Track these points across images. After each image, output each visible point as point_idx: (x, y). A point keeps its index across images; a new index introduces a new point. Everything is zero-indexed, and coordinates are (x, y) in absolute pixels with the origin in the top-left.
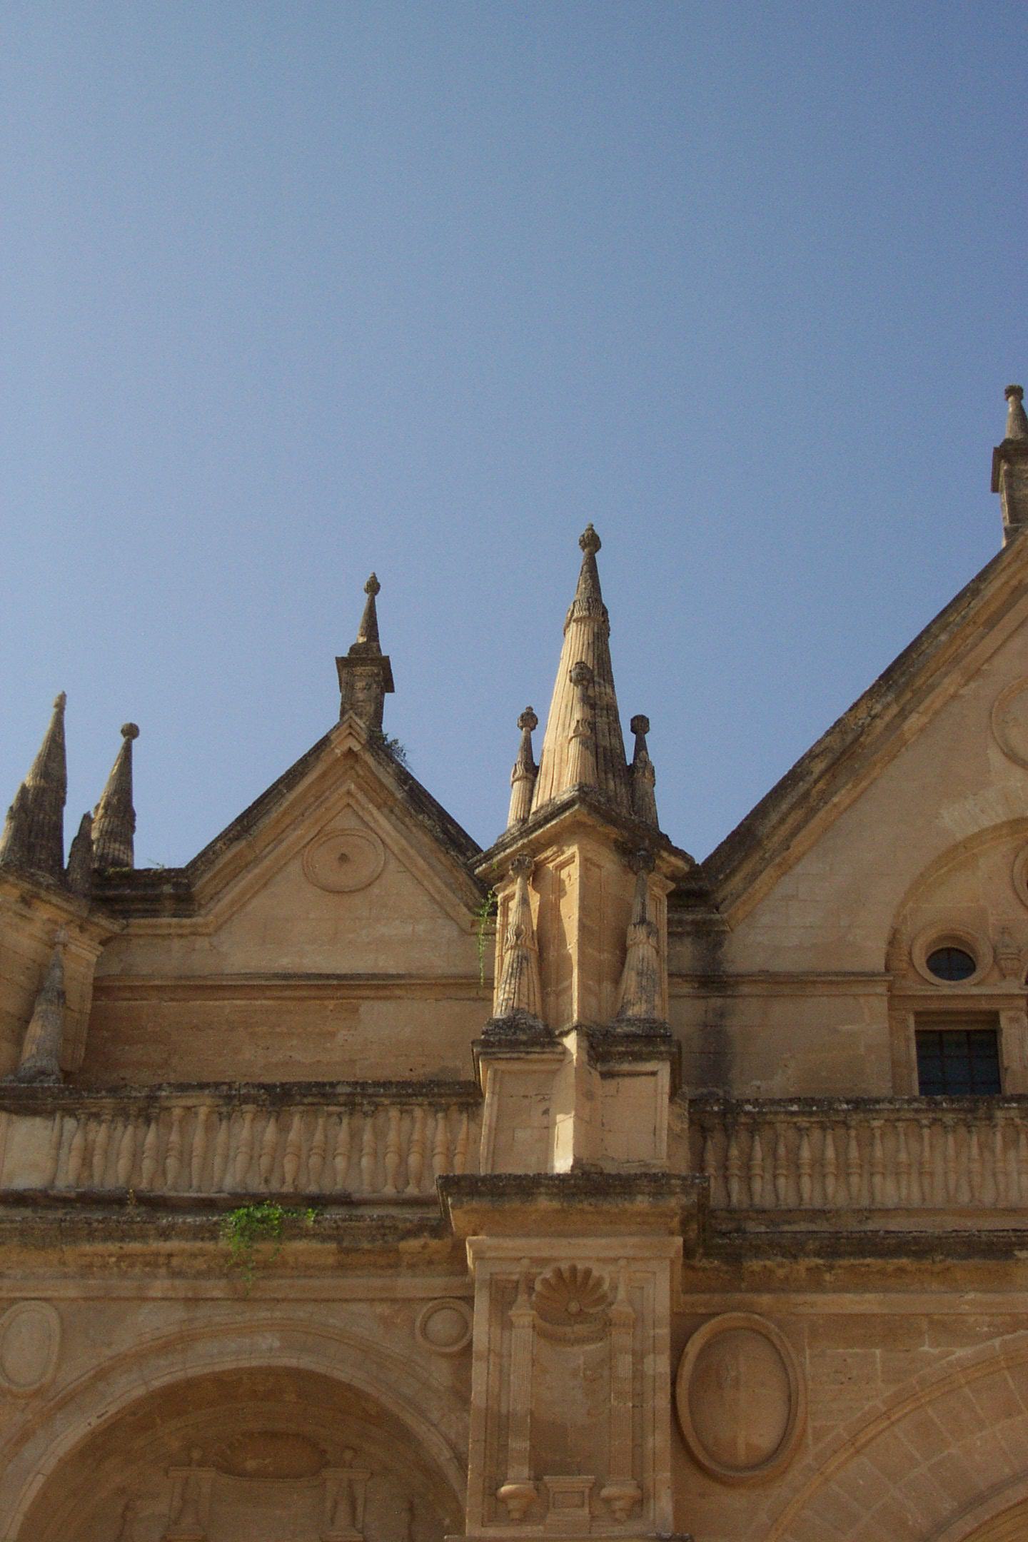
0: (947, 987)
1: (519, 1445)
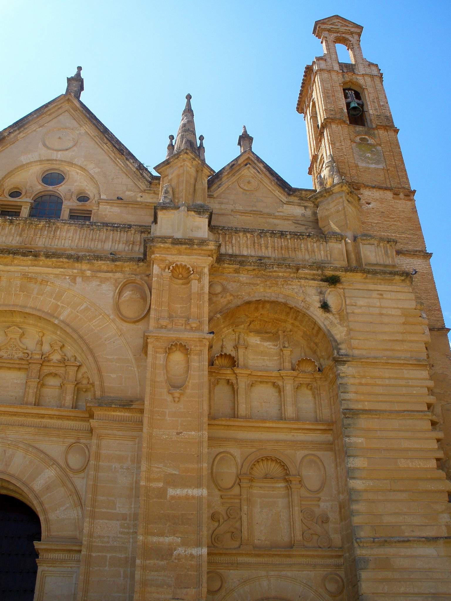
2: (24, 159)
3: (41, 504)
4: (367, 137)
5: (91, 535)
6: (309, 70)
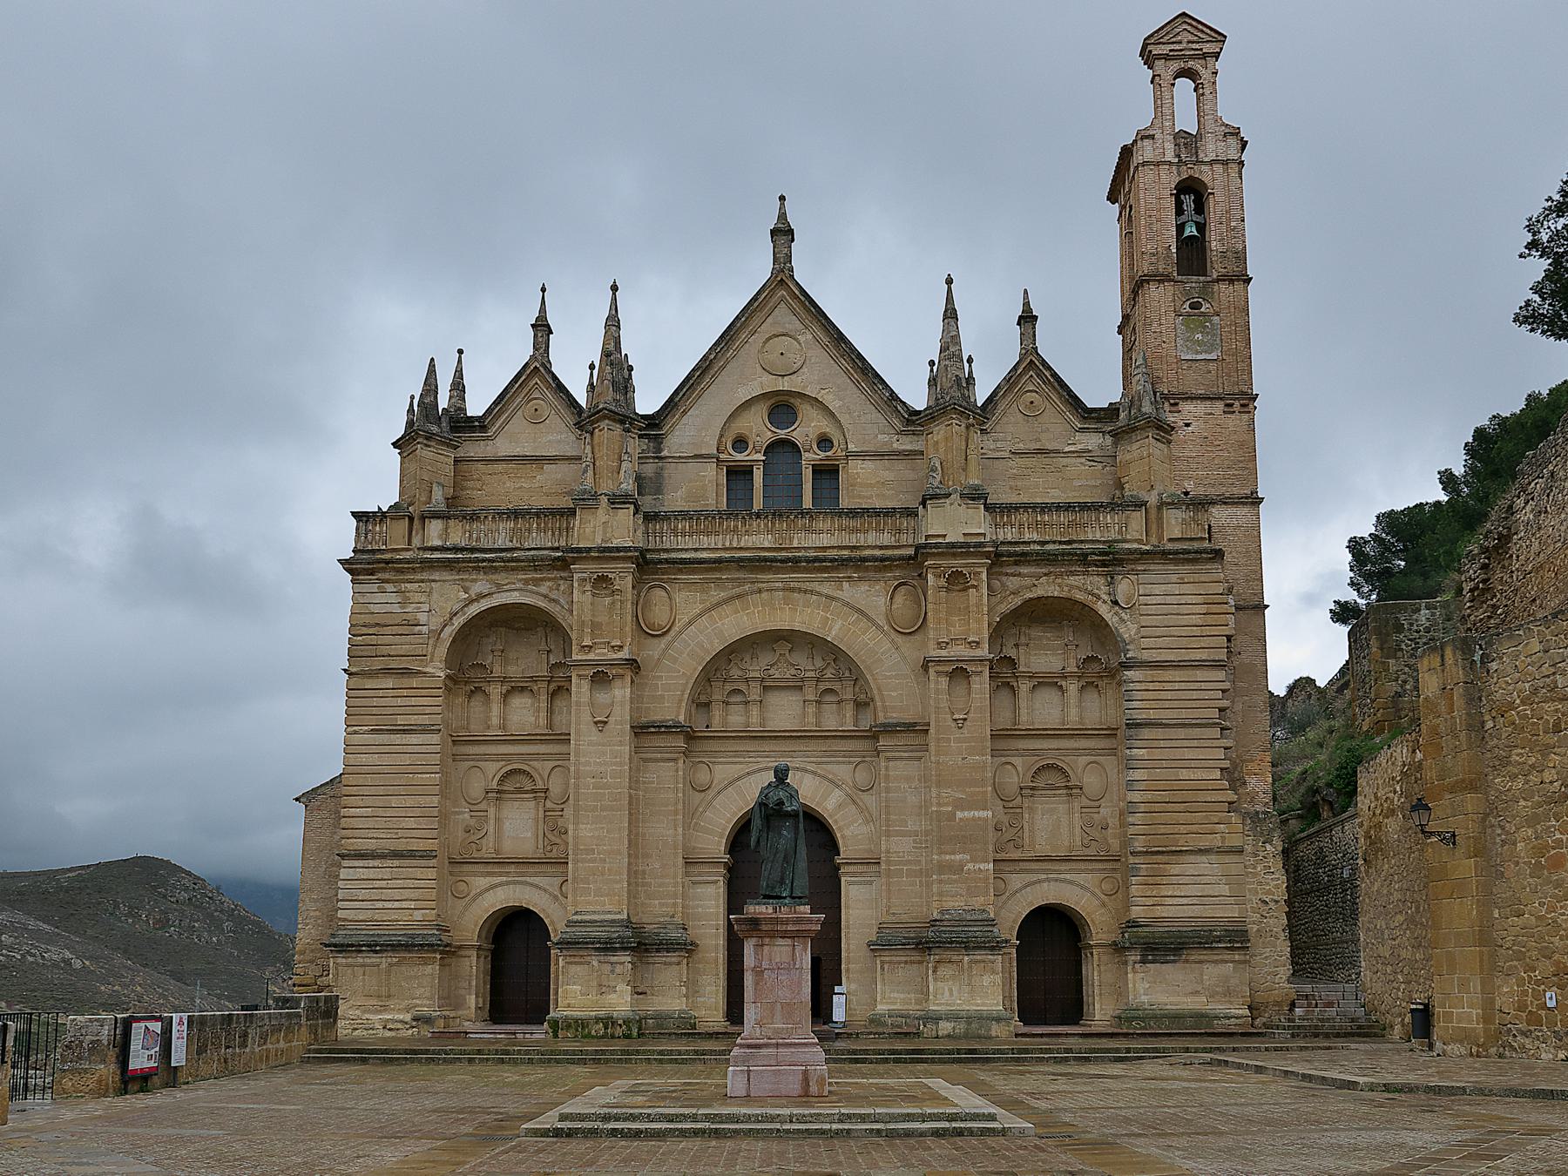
0: (739, 457)
2: (744, 394)
4: (1200, 300)
5: (888, 852)
6: (1126, 152)
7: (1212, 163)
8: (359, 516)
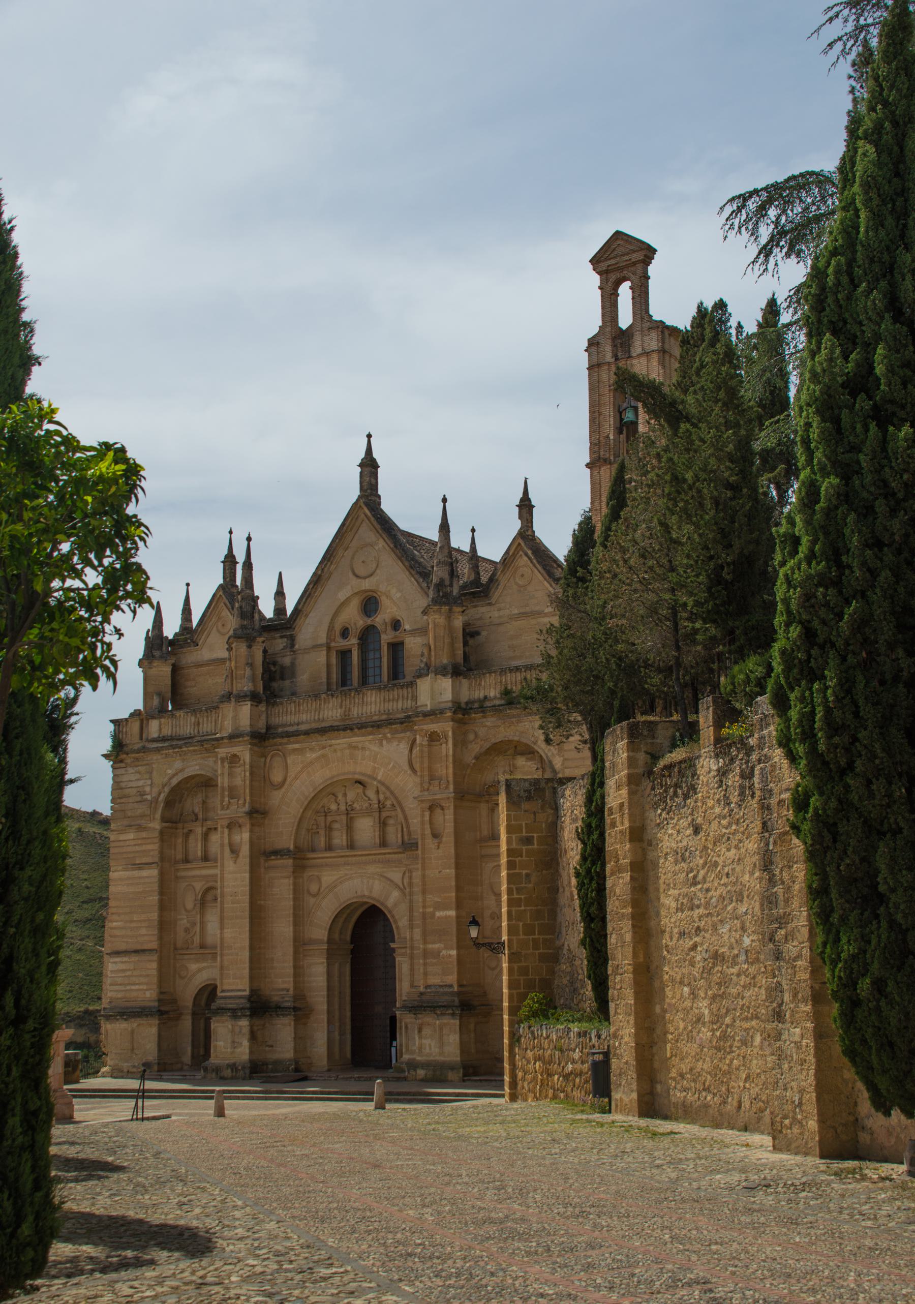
1: (226, 793)
2: (342, 596)
3: (393, 916)
7: (639, 356)
8: (112, 721)
